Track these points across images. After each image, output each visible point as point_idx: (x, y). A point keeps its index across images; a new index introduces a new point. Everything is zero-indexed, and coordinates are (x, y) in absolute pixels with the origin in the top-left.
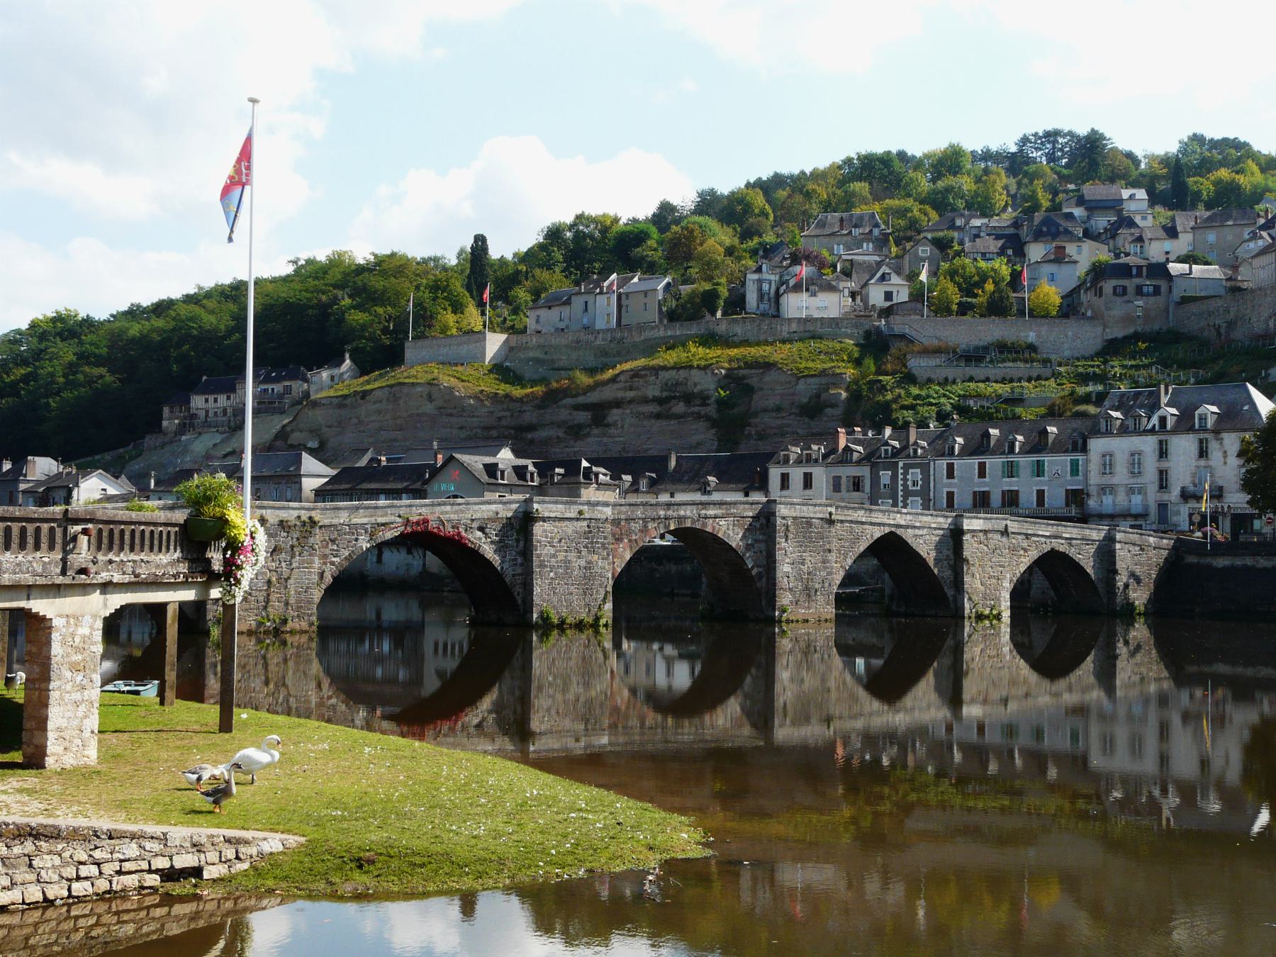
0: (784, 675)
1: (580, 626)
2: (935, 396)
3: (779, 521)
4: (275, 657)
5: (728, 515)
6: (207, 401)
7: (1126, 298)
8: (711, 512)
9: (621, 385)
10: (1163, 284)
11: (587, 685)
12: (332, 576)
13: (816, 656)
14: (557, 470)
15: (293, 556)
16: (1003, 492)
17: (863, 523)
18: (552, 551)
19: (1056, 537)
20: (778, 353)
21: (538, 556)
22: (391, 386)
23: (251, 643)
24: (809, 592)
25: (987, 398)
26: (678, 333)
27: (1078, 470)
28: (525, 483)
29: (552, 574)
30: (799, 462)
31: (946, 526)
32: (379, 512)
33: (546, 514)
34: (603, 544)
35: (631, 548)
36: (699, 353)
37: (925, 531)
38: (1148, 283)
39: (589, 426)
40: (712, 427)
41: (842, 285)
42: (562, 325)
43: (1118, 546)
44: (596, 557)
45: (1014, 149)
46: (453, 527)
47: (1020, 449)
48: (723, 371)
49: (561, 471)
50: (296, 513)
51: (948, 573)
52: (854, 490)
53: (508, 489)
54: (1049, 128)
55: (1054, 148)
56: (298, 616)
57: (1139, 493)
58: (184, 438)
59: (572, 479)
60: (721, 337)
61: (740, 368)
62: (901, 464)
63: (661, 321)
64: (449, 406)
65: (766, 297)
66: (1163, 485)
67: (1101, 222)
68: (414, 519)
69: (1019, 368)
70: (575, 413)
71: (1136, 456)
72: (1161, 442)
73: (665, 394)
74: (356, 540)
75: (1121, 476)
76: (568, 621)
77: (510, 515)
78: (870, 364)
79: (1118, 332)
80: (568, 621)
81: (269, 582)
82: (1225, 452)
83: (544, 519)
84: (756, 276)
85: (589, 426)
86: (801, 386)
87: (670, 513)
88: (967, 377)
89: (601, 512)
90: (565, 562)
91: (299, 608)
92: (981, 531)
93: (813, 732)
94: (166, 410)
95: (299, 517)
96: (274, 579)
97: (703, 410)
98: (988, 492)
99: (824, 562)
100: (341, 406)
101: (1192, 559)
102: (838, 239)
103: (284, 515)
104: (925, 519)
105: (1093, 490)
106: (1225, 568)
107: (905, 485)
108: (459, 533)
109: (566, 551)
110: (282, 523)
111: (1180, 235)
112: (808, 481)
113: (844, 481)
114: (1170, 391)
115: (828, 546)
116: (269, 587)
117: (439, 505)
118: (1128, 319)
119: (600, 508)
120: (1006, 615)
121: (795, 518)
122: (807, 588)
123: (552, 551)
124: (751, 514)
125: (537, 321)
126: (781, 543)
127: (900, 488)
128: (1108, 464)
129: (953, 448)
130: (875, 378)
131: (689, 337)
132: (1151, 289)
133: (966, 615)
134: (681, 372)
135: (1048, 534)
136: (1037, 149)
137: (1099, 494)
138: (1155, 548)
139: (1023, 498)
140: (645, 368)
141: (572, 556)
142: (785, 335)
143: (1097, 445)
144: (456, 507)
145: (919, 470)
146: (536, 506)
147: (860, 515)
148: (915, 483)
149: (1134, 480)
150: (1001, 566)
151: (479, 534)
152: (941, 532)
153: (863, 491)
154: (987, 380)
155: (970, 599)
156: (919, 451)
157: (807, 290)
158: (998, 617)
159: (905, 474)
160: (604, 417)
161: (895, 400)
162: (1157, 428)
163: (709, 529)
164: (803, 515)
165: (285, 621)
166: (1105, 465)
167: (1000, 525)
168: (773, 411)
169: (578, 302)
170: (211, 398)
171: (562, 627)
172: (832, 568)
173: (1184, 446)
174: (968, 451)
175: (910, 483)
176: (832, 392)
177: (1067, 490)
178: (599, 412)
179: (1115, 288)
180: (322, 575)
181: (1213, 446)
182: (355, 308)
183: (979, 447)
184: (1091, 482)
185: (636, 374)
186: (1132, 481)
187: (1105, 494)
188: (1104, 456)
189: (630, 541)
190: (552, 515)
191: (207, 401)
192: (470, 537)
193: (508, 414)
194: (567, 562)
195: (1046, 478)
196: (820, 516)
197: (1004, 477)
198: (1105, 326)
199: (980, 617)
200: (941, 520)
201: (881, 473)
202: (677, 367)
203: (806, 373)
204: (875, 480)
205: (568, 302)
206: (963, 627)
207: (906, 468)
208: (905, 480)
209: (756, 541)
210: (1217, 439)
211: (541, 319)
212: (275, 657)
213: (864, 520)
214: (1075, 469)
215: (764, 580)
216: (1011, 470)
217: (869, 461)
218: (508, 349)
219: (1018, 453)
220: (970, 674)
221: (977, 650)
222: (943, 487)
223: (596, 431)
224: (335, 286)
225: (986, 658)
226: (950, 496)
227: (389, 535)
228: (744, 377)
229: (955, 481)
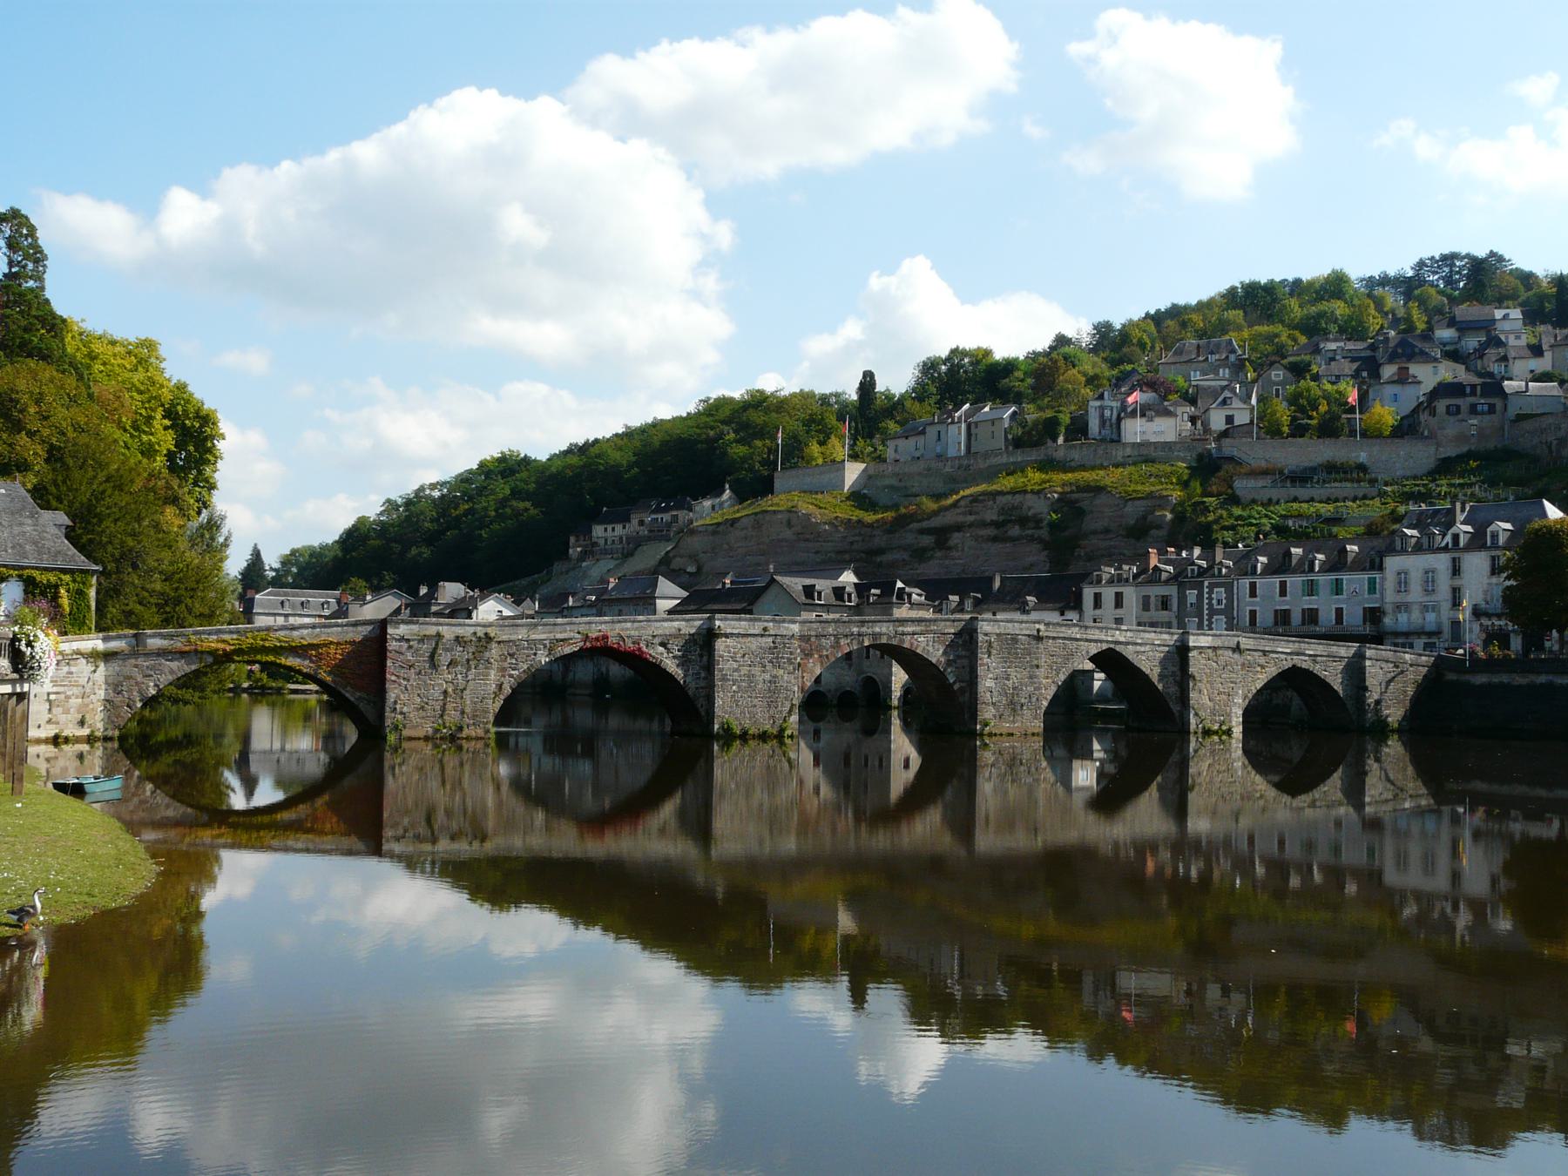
0: (986, 787)
1: (763, 737)
2: (1257, 516)
3: (981, 637)
5: (927, 632)
6: (606, 530)
7: (1460, 417)
8: (909, 629)
9: (962, 510)
10: (1498, 403)
12: (511, 687)
13: (1022, 768)
14: (873, 591)
15: (469, 669)
16: (1303, 610)
17: (1077, 640)
18: (735, 665)
19: (1298, 654)
20: (1108, 477)
21: (721, 670)
22: (756, 514)
23: (428, 749)
24: (1014, 707)
25: (1308, 517)
26: (1019, 459)
27: (1375, 588)
28: (842, 604)
29: (734, 688)
30: (1111, 582)
31: (1172, 643)
32: (558, 628)
33: (729, 631)
34: (789, 659)
35: (822, 663)
36: (1035, 476)
37: (1147, 648)
38: (1483, 401)
39: (933, 549)
40: (1044, 549)
41: (1180, 410)
42: (918, 454)
43: (1368, 663)
44: (781, 672)
45: (1410, 273)
46: (634, 643)
47: (1320, 568)
48: (1056, 495)
49: (877, 592)
50: (472, 630)
51: (1173, 689)
52: (1163, 609)
53: (825, 609)
54: (1446, 251)
55: (1451, 271)
56: (474, 724)
57: (1433, 611)
58: (584, 564)
59: (886, 600)
60: (1058, 462)
61: (1072, 492)
62: (1206, 583)
63: (1007, 448)
64: (805, 531)
65: (1108, 423)
67: (1472, 342)
68: (594, 635)
69: (1348, 488)
70: (920, 537)
71: (1430, 574)
72: (1454, 560)
73: (1001, 518)
74: (535, 654)
75: (1415, 594)
76: (750, 732)
77: (693, 631)
78: (1196, 486)
79: (1451, 451)
80: (750, 732)
81: (445, 692)
83: (727, 636)
84: (1098, 403)
85: (933, 549)
86: (1129, 508)
87: (864, 629)
88: (1292, 497)
89: (787, 629)
90: (749, 677)
91: (474, 717)
92: (1209, 648)
93: (1020, 842)
94: (572, 539)
95: (475, 633)
96: (450, 690)
97: (1037, 533)
98: (1289, 610)
99: (1031, 677)
100: (714, 533)
101: (1451, 676)
102: (1194, 365)
103: (460, 631)
104: (1147, 635)
105: (1389, 608)
106: (1481, 686)
107: (1210, 604)
108: (640, 649)
109: (750, 666)
110: (458, 640)
111: (1545, 354)
112: (1119, 601)
113: (1153, 599)
114: (1467, 509)
115: (1036, 662)
116: (445, 697)
117: (619, 622)
118: (1462, 438)
119: (786, 625)
120: (1238, 731)
121: (997, 635)
122: (1012, 703)
123: (735, 665)
124: (953, 631)
125: (896, 451)
126: (983, 658)
127: (1206, 607)
128: (1403, 582)
129: (1256, 567)
130: (1200, 499)
131: (1028, 463)
132: (1486, 408)
133: (1192, 730)
134: (1017, 496)
135: (1288, 651)
136: (1435, 273)
137: (1394, 611)
138: (1411, 665)
139: (1322, 616)
140: (983, 493)
141: (757, 670)
142: (1120, 459)
143: (1393, 563)
144: (636, 624)
145: (1223, 589)
146: (718, 623)
148: (1219, 602)
149: (1428, 598)
150: (1232, 682)
152: (1167, 649)
153: (1171, 610)
154: (1312, 500)
155: (1196, 714)
156: (1224, 570)
157: (1143, 415)
158: (1229, 732)
159: (1210, 593)
160: (947, 540)
161: (1216, 521)
162: (1450, 546)
163: (906, 645)
164: (1007, 631)
165: (460, 729)
166: (1400, 583)
167: (1233, 642)
168: (1102, 533)
169: (932, 432)
170: (610, 528)
171: (744, 737)
172: (1040, 683)
174: (1269, 570)
175: (1214, 602)
176: (1158, 514)
177: (1364, 609)
178: (942, 535)
179: (1448, 407)
180: (500, 687)
182: (737, 441)
183: (1281, 565)
184: (1387, 600)
185: (975, 499)
186: (1426, 599)
188: (1399, 574)
189: (821, 656)
190: (735, 631)
191: (606, 530)
192: (651, 652)
193: (860, 538)
194: (750, 676)
195: (1345, 596)
196: (1028, 632)
197: (1303, 595)
198: (1438, 445)
199: (1207, 733)
200: (1166, 637)
201: (1188, 592)
202: (1013, 492)
203: (1134, 495)
204: (1182, 599)
205: (923, 432)
206: (1189, 742)
207: (1211, 586)
208: (1210, 599)
209: (959, 657)
211: (899, 449)
212: (451, 761)
213: (1078, 636)
214: (1372, 589)
215: (967, 695)
216: (1311, 588)
217: (1177, 580)
218: (866, 477)
219: (1318, 572)
220: (1196, 789)
222: (1245, 605)
223: (938, 554)
224: (723, 422)
225: (1215, 773)
226: (1253, 614)
227: (568, 650)
228: (1077, 501)
229: (1258, 599)
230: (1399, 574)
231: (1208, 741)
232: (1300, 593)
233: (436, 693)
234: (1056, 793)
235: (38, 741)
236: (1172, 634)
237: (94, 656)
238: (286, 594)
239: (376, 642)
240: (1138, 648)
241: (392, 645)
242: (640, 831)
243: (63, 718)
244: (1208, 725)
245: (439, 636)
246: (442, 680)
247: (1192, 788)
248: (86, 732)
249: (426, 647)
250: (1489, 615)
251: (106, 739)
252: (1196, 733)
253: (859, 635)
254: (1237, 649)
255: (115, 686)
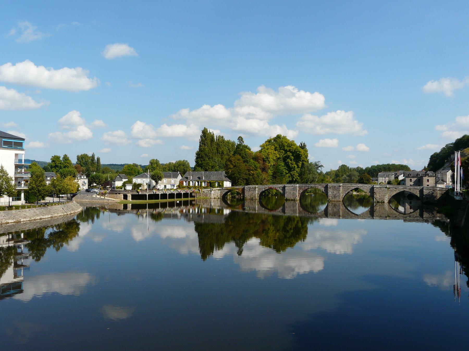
1: (292, 200)
3: (328, 186)
4: (252, 202)
8: (317, 185)
11: (293, 207)
19: (405, 188)
24: (335, 197)
37: (366, 188)
43: (424, 190)
44: (295, 191)
83: (287, 187)
87: (309, 185)
91: (254, 197)
103: (252, 187)
104: (365, 185)
121: (332, 186)
126: (329, 189)
138: (439, 190)
147: (349, 185)
151: (279, 188)
155: (376, 199)
158: (384, 202)
165: (253, 198)
171: (289, 200)
199: (378, 202)
212: (252, 202)
220: (376, 212)
221: (378, 208)
225: (381, 209)
227: (267, 189)
231: (378, 204)
233: (250, 194)
234: (346, 211)
235: (212, 198)
236: (372, 185)
237: (218, 190)
238: (385, 173)
239: (244, 188)
240: (364, 188)
241: (245, 188)
242: (276, 211)
243: (215, 196)
244: (378, 200)
245: (250, 187)
246: (251, 192)
247: (375, 212)
248: (218, 197)
249: (249, 189)
251: (220, 198)
252: (375, 202)
253: (309, 186)
254: (386, 188)
255: (221, 193)
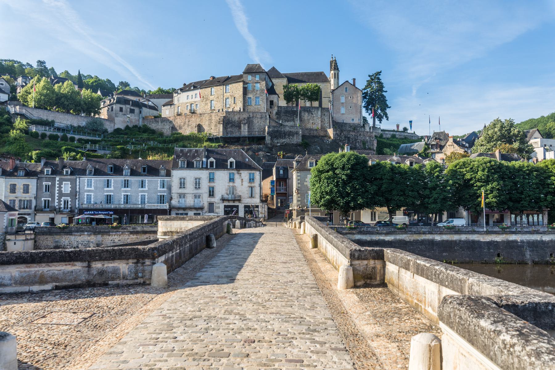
62: (57, 179)
66: (211, 193)
72: (210, 174)
75: (190, 188)
82: (242, 180)
127: (57, 192)
128: (182, 185)
145: (69, 183)
159: (60, 184)
173: (222, 176)
181: (237, 176)
187: (180, 197)
208: (60, 187)
210: (238, 174)
230: (180, 179)
232: (120, 186)
250: (228, 200)
